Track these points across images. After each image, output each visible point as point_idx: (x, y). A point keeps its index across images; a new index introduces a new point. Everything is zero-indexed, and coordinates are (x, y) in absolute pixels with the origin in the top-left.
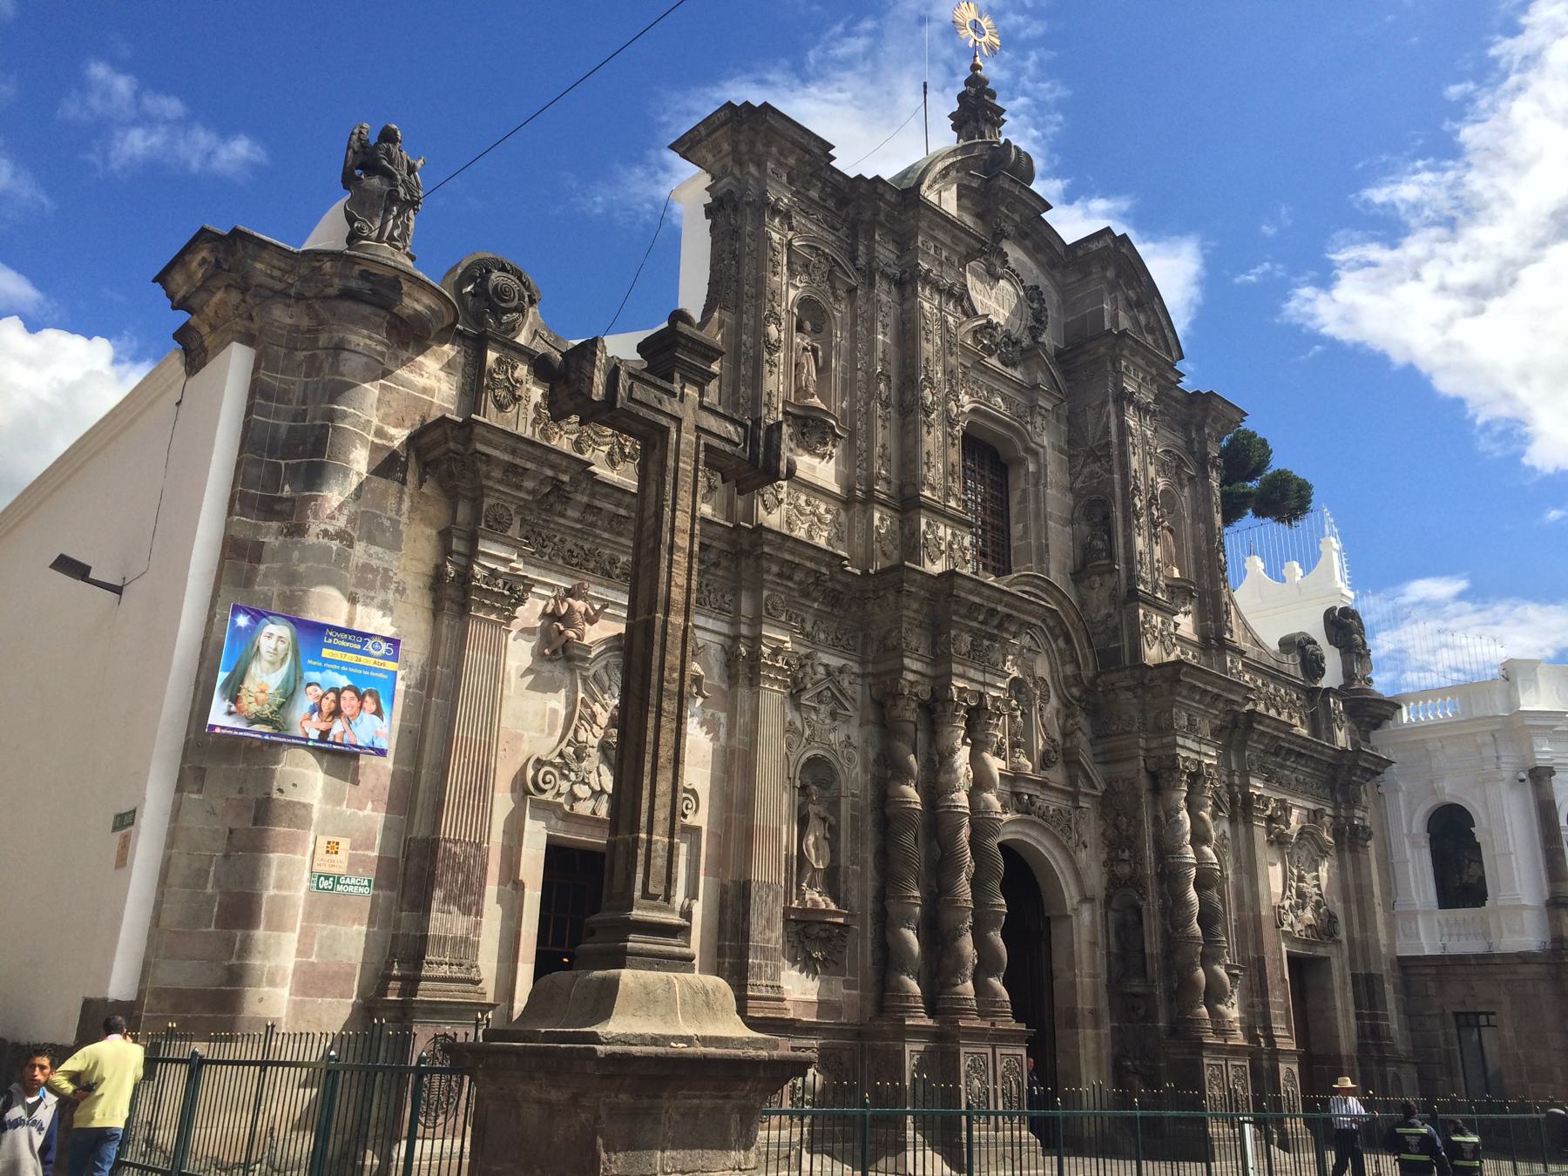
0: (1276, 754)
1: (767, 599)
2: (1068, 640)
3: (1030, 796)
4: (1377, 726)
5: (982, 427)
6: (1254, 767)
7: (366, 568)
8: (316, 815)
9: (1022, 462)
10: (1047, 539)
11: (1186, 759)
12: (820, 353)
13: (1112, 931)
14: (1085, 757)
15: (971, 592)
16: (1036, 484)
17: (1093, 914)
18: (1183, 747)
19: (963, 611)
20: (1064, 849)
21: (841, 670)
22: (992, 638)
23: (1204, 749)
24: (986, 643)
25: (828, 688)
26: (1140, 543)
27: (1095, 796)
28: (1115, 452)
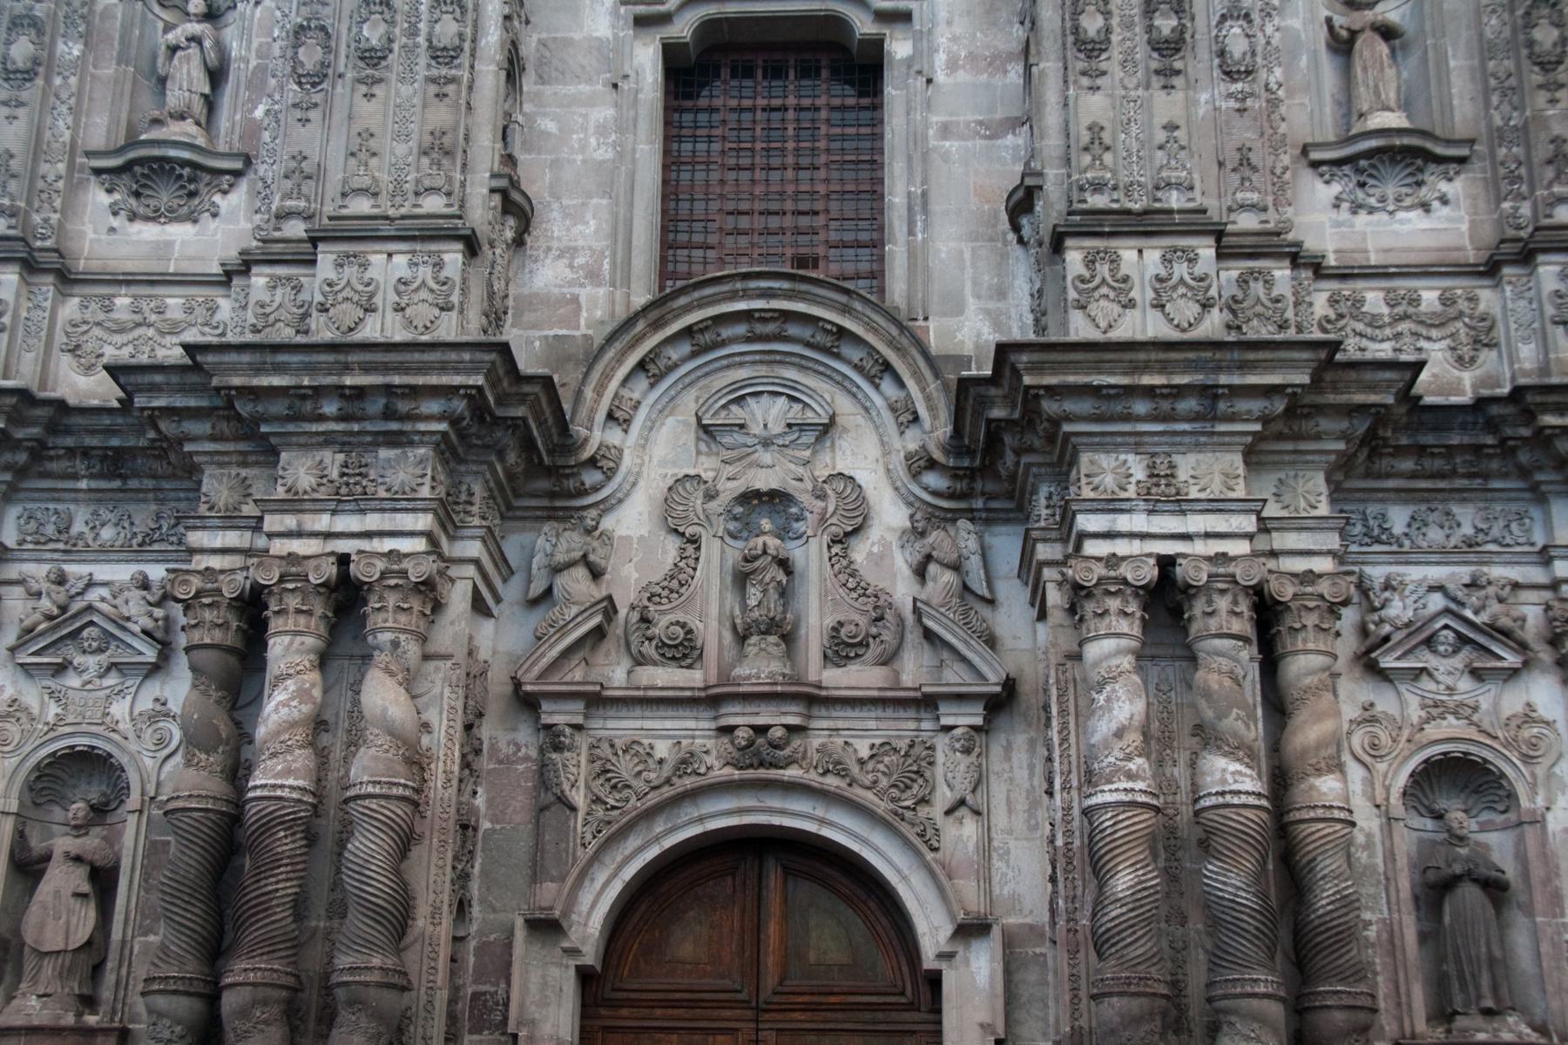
2: (901, 384)
3: (761, 730)
9: (876, 47)
10: (925, 181)
15: (259, 370)
17: (992, 960)
19: (279, 407)
22: (395, 440)
23: (1196, 523)
25: (92, 623)
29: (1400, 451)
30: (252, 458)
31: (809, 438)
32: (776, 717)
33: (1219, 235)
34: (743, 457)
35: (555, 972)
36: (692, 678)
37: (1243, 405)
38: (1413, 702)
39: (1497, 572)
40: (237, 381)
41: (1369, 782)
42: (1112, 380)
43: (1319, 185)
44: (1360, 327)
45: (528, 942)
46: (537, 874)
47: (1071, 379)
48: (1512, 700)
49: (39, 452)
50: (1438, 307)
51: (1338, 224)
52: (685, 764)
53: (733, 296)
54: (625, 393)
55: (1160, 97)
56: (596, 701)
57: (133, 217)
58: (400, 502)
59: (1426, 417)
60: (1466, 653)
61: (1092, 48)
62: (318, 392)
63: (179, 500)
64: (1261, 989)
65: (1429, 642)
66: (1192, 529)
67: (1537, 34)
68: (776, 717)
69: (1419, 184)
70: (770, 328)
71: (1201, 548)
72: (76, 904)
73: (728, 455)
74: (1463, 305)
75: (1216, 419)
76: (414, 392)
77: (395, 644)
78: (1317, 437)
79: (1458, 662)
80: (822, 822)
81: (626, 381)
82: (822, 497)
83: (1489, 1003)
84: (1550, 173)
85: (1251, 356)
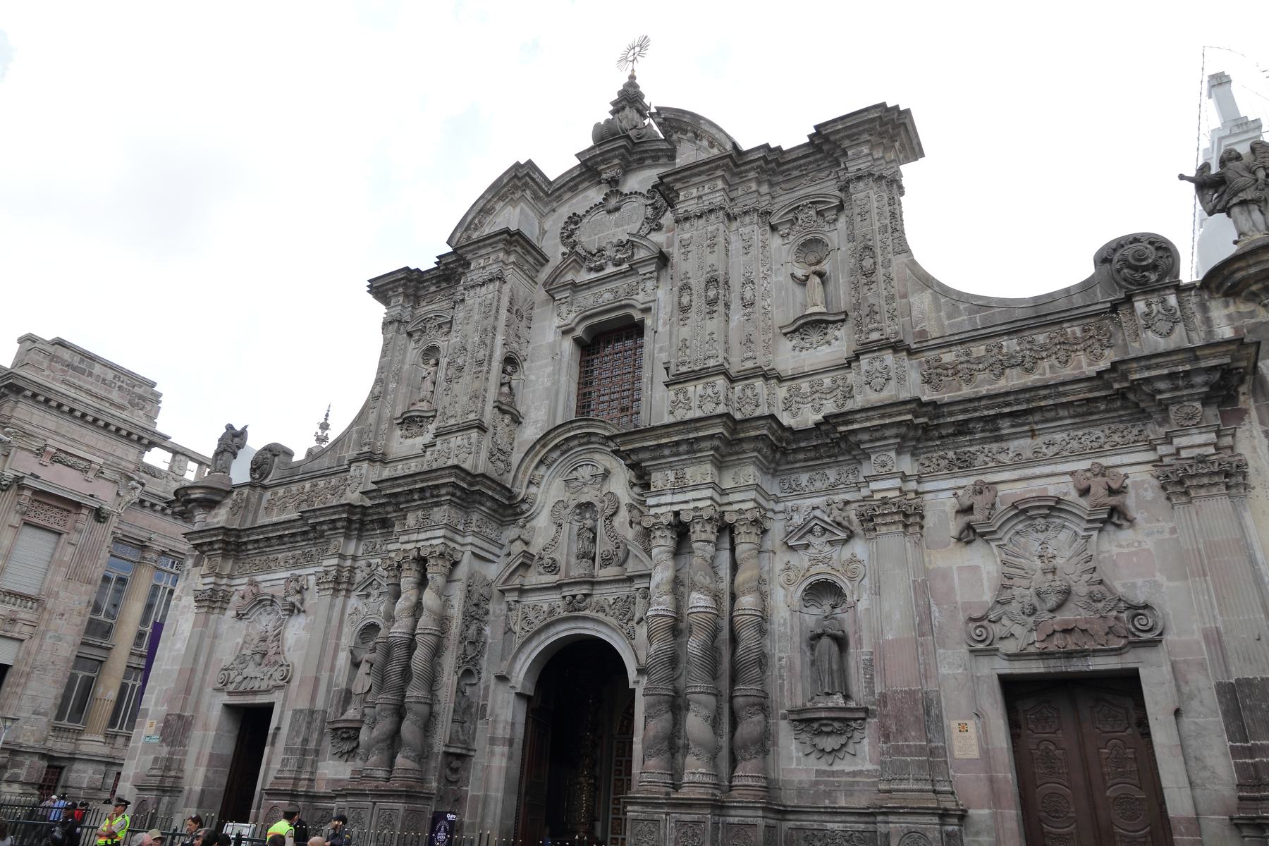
3: (574, 597)
7: (185, 607)
8: (150, 712)
9: (643, 321)
15: (394, 487)
18: (658, 505)
19: (402, 499)
22: (437, 504)
23: (689, 496)
29: (795, 451)
31: (599, 479)
32: (579, 591)
33: (726, 374)
34: (578, 490)
35: (506, 695)
36: (557, 577)
37: (704, 445)
38: (806, 558)
39: (837, 498)
40: (388, 492)
41: (786, 596)
42: (651, 443)
43: (788, 343)
44: (798, 399)
45: (496, 684)
46: (503, 658)
47: (637, 445)
48: (846, 552)
49: (362, 523)
50: (830, 385)
51: (794, 357)
52: (552, 612)
53: (569, 431)
54: (537, 473)
55: (708, 322)
56: (522, 591)
57: (406, 438)
58: (438, 526)
59: (797, 436)
60: (827, 537)
61: (685, 309)
62: (411, 491)
64: (698, 690)
65: (811, 531)
66: (687, 499)
67: (864, 263)
68: (579, 591)
69: (825, 334)
70: (585, 440)
71: (691, 505)
72: (366, 677)
73: (572, 490)
74: (840, 382)
75: (695, 452)
76: (437, 487)
77: (433, 578)
78: (744, 452)
79: (824, 539)
80: (597, 631)
81: (537, 467)
82: (603, 501)
83: (827, 690)
84: (868, 319)
85: (698, 425)
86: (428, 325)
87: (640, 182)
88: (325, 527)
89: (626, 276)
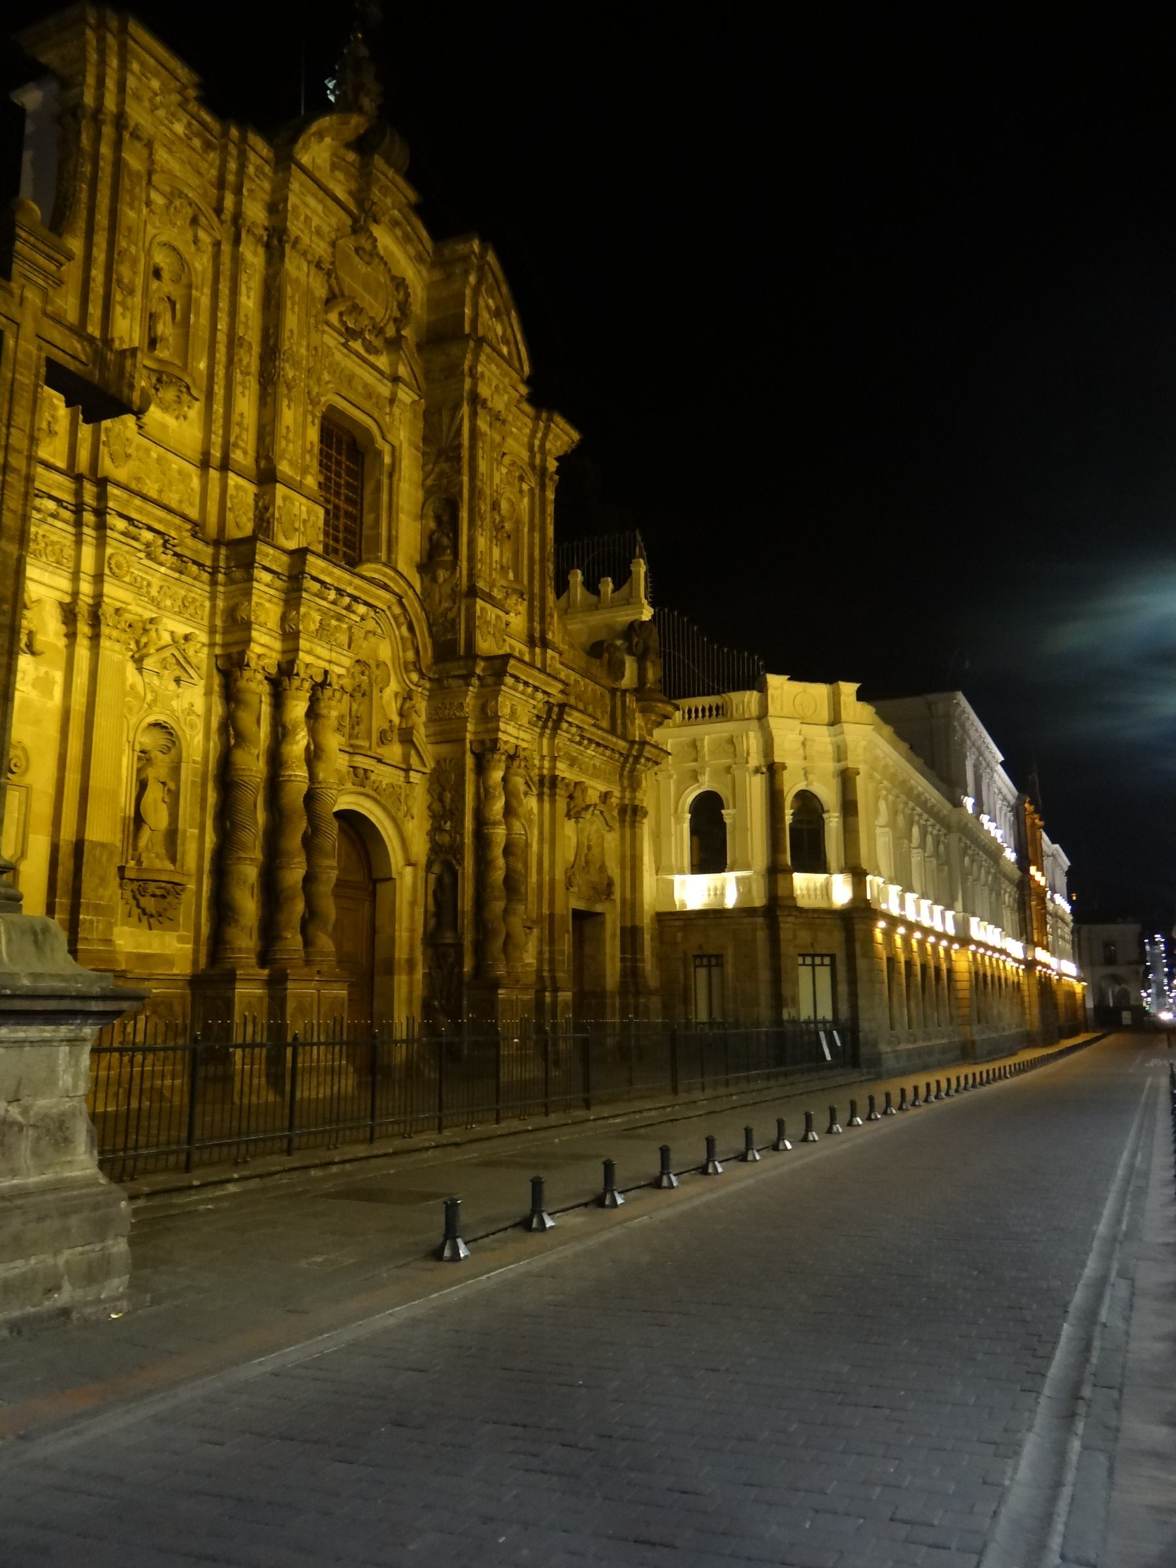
0: (580, 743)
1: (110, 558)
3: (365, 770)
4: (660, 724)
5: (343, 414)
6: (561, 754)
10: (397, 532)
11: (506, 742)
12: (178, 307)
13: (430, 892)
14: (421, 735)
16: (391, 476)
17: (415, 877)
18: (504, 732)
20: (393, 819)
21: (187, 638)
22: (340, 618)
23: (522, 735)
24: (334, 623)
26: (482, 543)
27: (424, 773)
28: (465, 453)
30: (274, 600)
63: (196, 593)
86: (177, 203)
87: (386, 248)
88: (121, 524)
89: (380, 381)
